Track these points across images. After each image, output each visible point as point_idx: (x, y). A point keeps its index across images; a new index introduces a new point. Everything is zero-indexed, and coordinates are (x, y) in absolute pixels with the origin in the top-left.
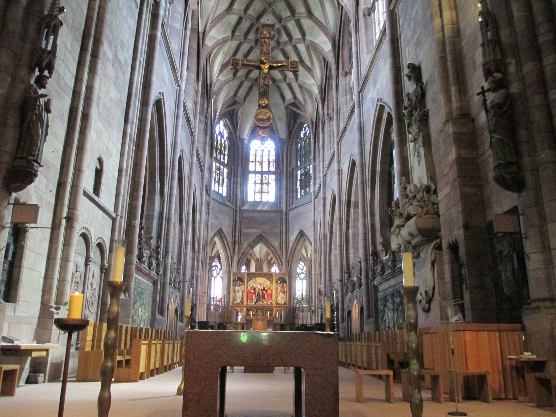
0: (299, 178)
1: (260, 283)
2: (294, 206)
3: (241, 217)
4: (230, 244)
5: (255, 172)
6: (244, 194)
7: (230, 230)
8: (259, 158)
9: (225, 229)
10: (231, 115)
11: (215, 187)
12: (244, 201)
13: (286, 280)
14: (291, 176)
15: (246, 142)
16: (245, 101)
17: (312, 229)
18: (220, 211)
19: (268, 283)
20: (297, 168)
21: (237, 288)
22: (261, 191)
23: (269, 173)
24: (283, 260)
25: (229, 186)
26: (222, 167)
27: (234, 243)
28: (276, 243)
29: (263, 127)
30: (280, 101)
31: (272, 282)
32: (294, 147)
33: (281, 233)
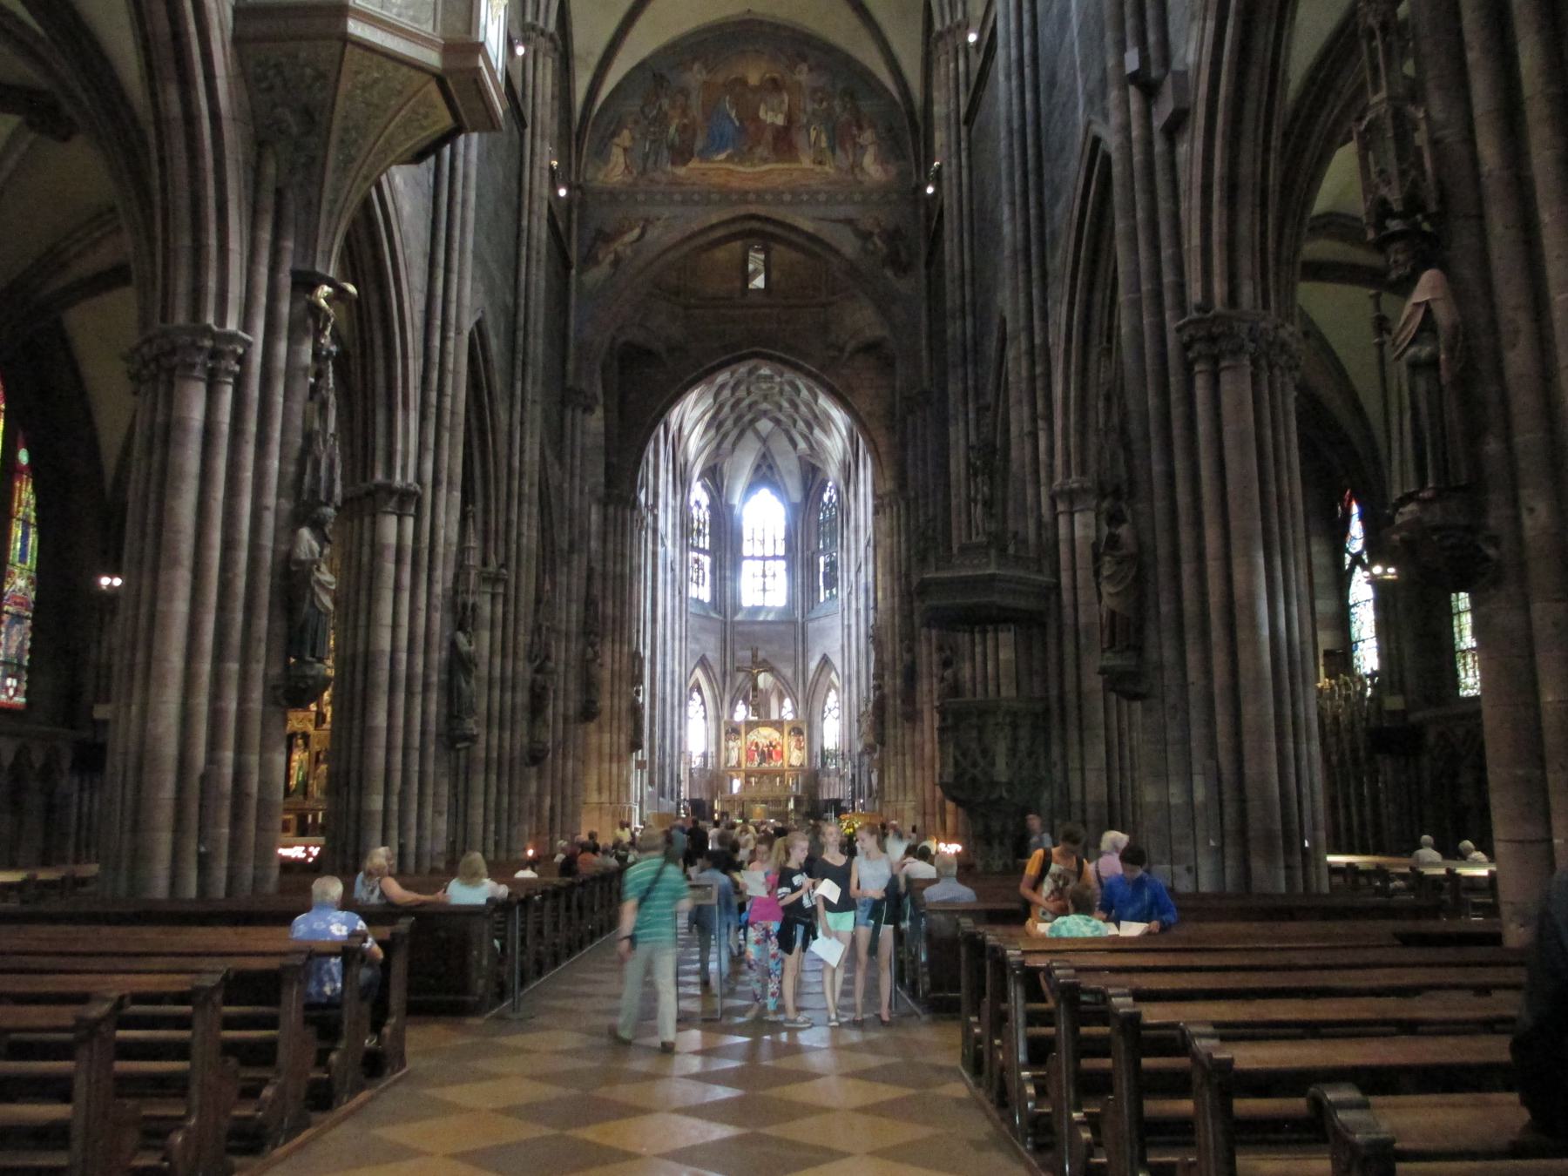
0: (822, 569)
1: (765, 735)
2: (813, 615)
3: (732, 633)
4: (718, 676)
5: (753, 558)
6: (736, 595)
7: (717, 655)
8: (758, 536)
9: (709, 655)
10: (714, 476)
11: (694, 591)
12: (737, 608)
13: (804, 729)
14: (810, 565)
15: (736, 511)
16: (733, 450)
17: (839, 655)
18: (703, 629)
19: (775, 735)
20: (818, 552)
21: (731, 744)
22: (764, 587)
23: (775, 557)
24: (800, 697)
25: (713, 585)
26: (701, 556)
27: (724, 674)
28: (788, 672)
29: (765, 473)
30: (790, 448)
31: (782, 733)
32: (813, 517)
33: (795, 658)
